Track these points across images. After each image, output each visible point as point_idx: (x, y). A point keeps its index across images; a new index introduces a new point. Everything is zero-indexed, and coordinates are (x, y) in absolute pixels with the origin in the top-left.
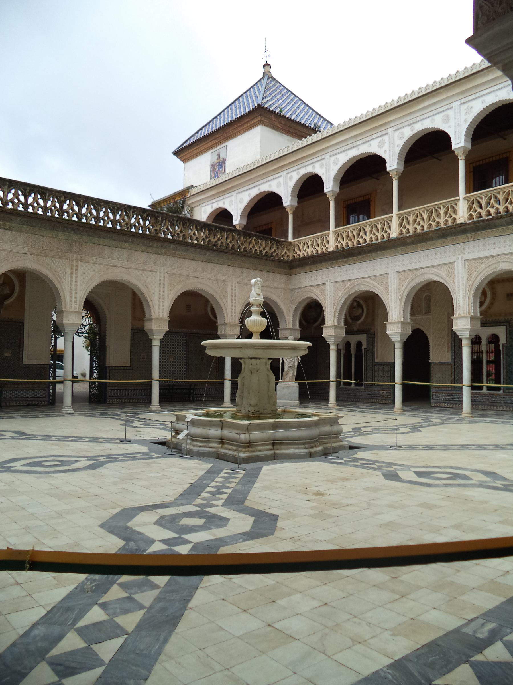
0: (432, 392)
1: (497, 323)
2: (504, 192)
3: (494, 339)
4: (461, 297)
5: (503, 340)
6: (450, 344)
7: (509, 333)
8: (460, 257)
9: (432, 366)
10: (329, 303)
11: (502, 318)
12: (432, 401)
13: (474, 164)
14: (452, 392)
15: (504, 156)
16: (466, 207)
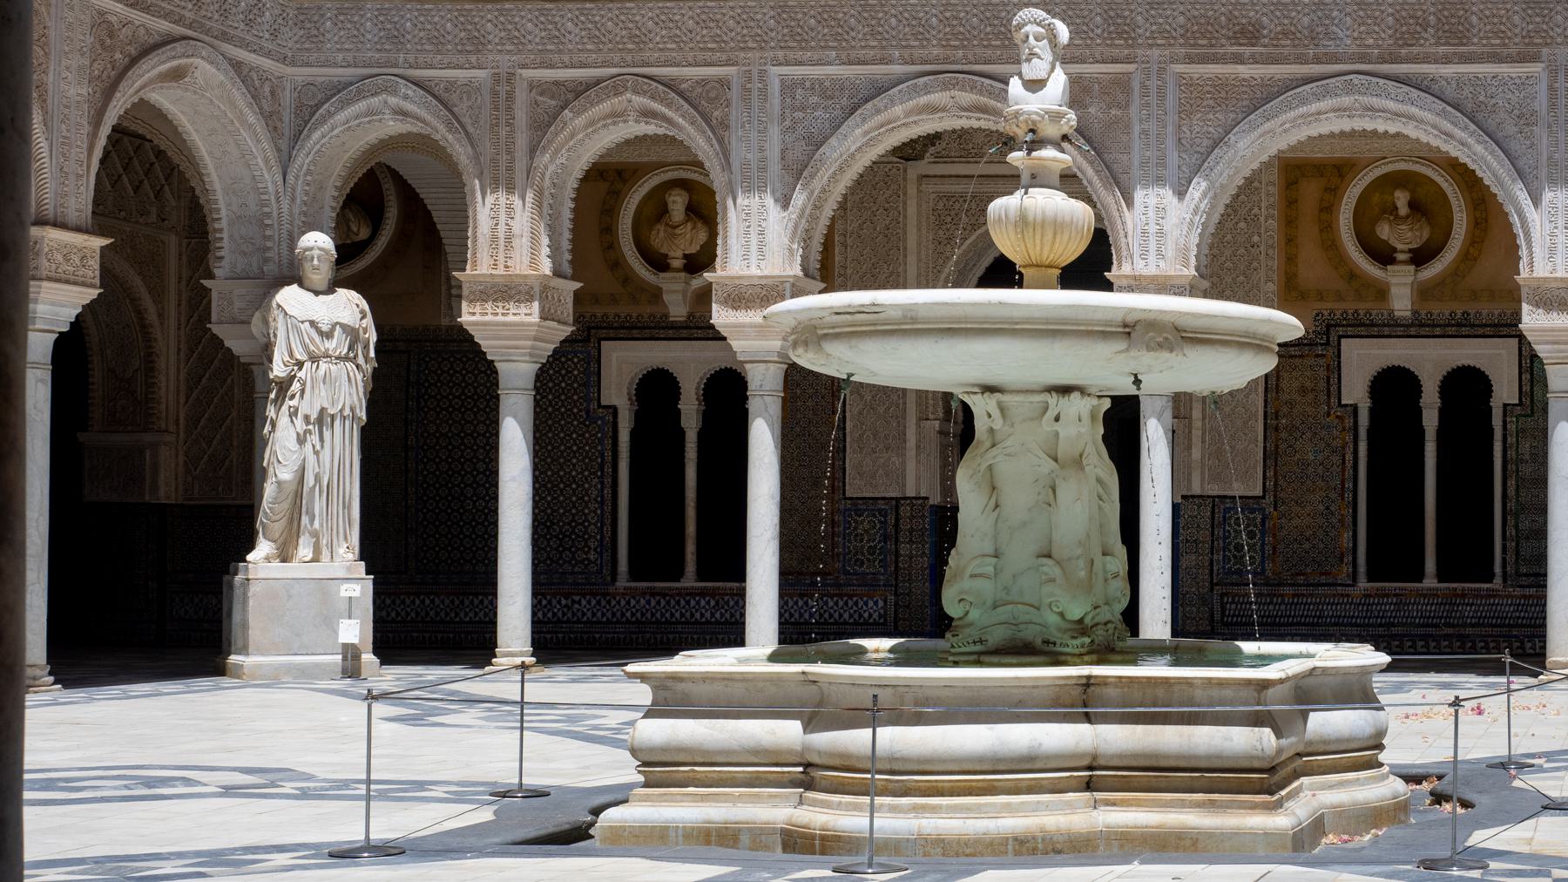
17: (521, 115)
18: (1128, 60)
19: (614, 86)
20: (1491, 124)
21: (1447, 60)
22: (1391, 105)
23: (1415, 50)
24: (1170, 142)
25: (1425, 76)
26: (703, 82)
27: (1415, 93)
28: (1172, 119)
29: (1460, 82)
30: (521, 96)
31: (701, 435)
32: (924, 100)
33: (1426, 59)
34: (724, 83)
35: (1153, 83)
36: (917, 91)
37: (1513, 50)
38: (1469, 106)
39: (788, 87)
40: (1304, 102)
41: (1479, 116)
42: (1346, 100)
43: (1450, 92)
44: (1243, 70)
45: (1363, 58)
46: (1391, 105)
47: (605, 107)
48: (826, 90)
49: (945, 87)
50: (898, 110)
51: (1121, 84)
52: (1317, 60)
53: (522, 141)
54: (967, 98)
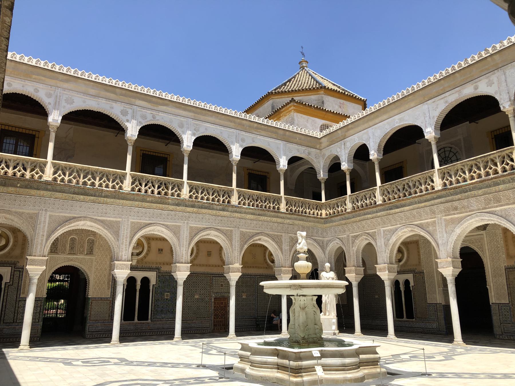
0: (88, 324)
1: (150, 269)
2: (212, 189)
3: (145, 281)
4: (184, 250)
5: (153, 281)
6: (111, 283)
7: (158, 277)
8: (186, 222)
9: (90, 301)
10: (41, 233)
11: (154, 266)
12: (87, 333)
13: (145, 152)
14: (108, 324)
15: (166, 156)
16: (188, 189)
17: (351, 242)
18: (435, 218)
19: (361, 235)
20: (510, 219)
21: (497, 207)
22: (487, 218)
23: (490, 206)
24: (444, 232)
25: (493, 211)
26: (373, 232)
27: (491, 215)
28: (444, 228)
29: (501, 210)
30: (350, 239)
31: (405, 291)
32: (403, 231)
33: (492, 207)
34: (375, 232)
35: (440, 221)
36: (401, 229)
37: (512, 202)
38: (504, 216)
39: (384, 231)
40: (468, 220)
41: (507, 218)
42: (477, 219)
43: (500, 214)
44: (456, 216)
45: (479, 209)
46: (487, 218)
47: (360, 239)
48: (388, 231)
49: (406, 227)
50: (400, 233)
51: (434, 222)
52: (470, 211)
53: (351, 246)
54: (410, 229)
